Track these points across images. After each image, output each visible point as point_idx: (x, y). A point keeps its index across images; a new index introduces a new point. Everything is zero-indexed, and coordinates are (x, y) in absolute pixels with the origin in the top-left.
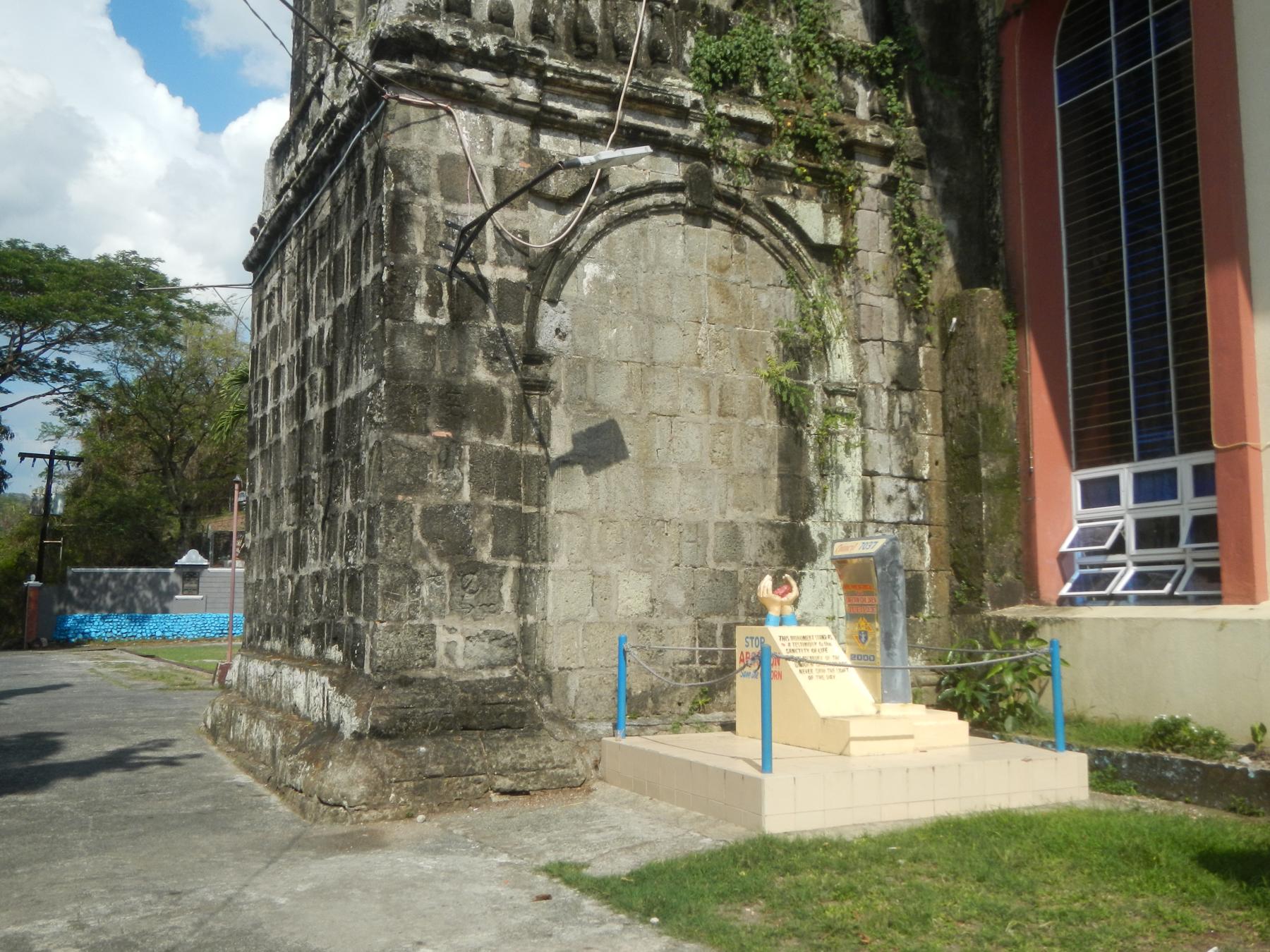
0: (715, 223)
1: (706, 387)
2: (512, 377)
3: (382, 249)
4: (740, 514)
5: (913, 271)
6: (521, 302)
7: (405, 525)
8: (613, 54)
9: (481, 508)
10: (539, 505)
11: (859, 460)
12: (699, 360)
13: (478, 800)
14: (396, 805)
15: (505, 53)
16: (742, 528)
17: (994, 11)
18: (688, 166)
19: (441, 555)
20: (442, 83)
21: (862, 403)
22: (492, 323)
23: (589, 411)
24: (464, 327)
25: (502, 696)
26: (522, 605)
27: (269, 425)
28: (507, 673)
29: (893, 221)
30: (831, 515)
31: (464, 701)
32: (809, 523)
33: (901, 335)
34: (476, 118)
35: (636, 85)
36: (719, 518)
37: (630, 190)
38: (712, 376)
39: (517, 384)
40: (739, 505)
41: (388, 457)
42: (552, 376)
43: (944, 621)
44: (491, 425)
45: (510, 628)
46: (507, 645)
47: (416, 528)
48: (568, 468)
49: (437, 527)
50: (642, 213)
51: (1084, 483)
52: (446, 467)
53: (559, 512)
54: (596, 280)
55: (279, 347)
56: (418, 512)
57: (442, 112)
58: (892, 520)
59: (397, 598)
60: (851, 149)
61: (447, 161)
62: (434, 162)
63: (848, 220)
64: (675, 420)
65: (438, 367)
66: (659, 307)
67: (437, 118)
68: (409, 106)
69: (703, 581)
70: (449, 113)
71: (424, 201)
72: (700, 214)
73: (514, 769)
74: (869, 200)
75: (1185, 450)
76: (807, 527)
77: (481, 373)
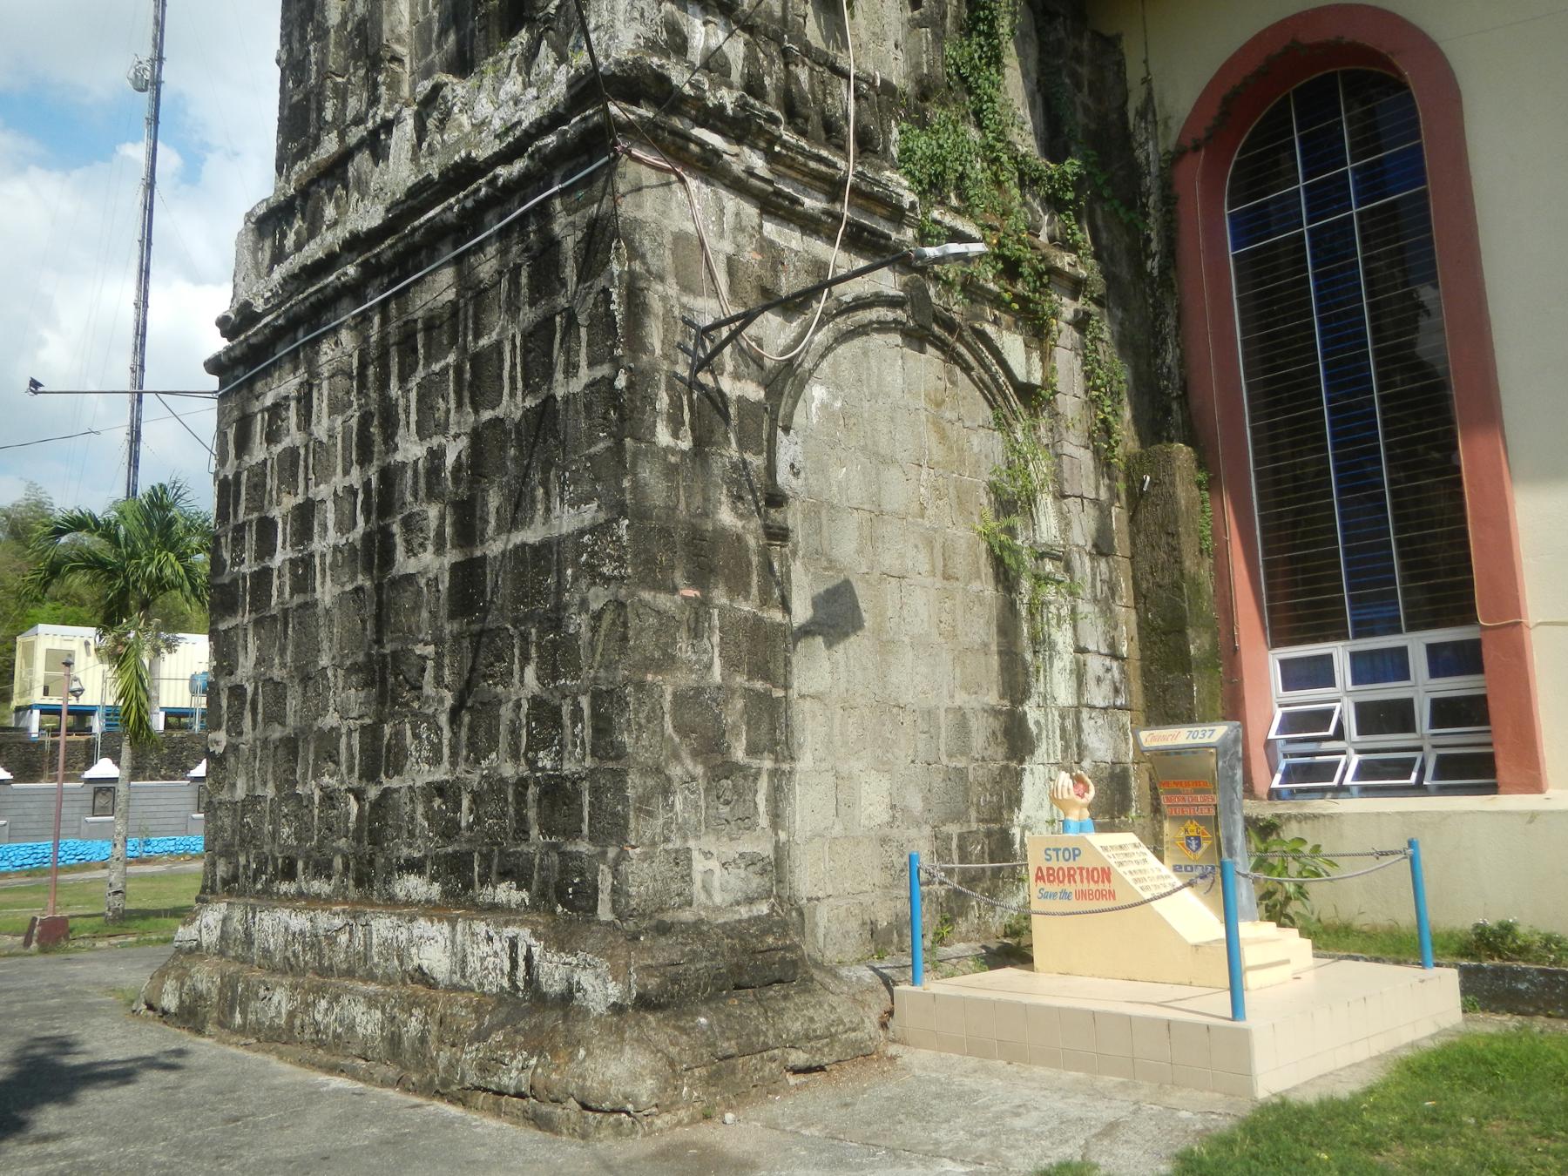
0: (929, 349)
1: (930, 543)
2: (756, 522)
3: (614, 346)
4: (965, 697)
5: (1104, 421)
6: (760, 427)
7: (655, 716)
8: (823, 136)
9: (733, 692)
11: (1069, 633)
12: (923, 508)
13: (771, 1087)
14: (689, 1104)
15: (742, 115)
16: (969, 715)
17: (1156, 145)
18: (905, 278)
19: (695, 754)
20: (680, 141)
21: (1068, 568)
22: (733, 451)
23: (826, 569)
24: (706, 454)
25: (770, 940)
26: (776, 818)
28: (763, 908)
29: (1084, 364)
30: (1045, 698)
31: (732, 949)
32: (1026, 708)
33: (1097, 493)
34: (706, 189)
35: (860, 175)
36: (947, 703)
37: (856, 299)
38: (935, 530)
39: (761, 531)
40: (965, 688)
41: (633, 623)
42: (790, 523)
43: (1148, 820)
44: (738, 586)
45: (766, 849)
46: (763, 872)
47: (667, 718)
48: (810, 639)
49: (689, 716)
50: (862, 330)
51: (1283, 663)
52: (696, 637)
53: (802, 696)
54: (824, 406)
56: (668, 697)
57: (674, 178)
58: (1102, 704)
59: (650, 814)
60: (1050, 275)
61: (680, 238)
62: (667, 239)
63: (1046, 357)
64: (904, 582)
65: (682, 505)
67: (668, 184)
68: (639, 167)
69: (938, 782)
70: (682, 180)
71: (660, 288)
72: (917, 337)
73: (808, 1038)
74: (1065, 335)
75: (1412, 628)
76: (1025, 713)
77: (726, 516)
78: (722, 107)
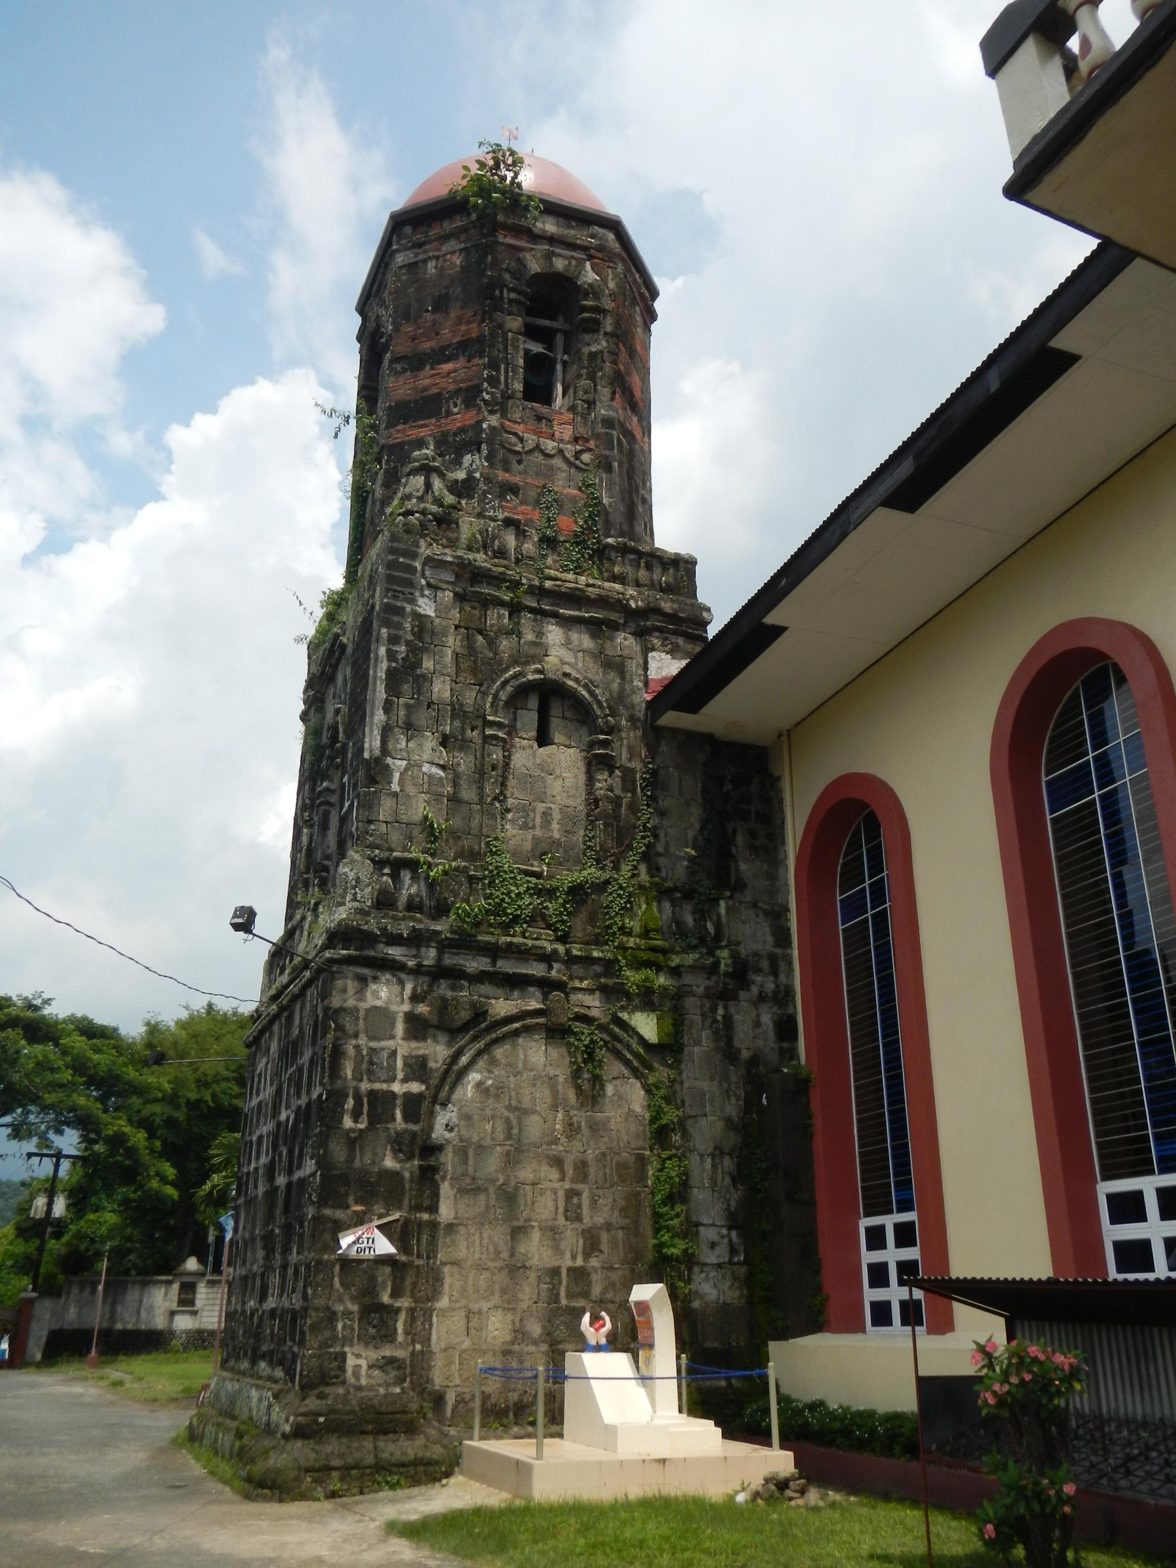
10: (428, 1258)
19: (353, 1299)
27: (251, 1181)
36: (569, 1263)
38: (566, 1151)
47: (336, 1279)
50: (516, 1033)
54: (479, 1085)
55: (262, 1120)
58: (715, 1261)
66: (526, 1102)
71: (354, 1042)
77: (389, 1163)
78: (401, 935)
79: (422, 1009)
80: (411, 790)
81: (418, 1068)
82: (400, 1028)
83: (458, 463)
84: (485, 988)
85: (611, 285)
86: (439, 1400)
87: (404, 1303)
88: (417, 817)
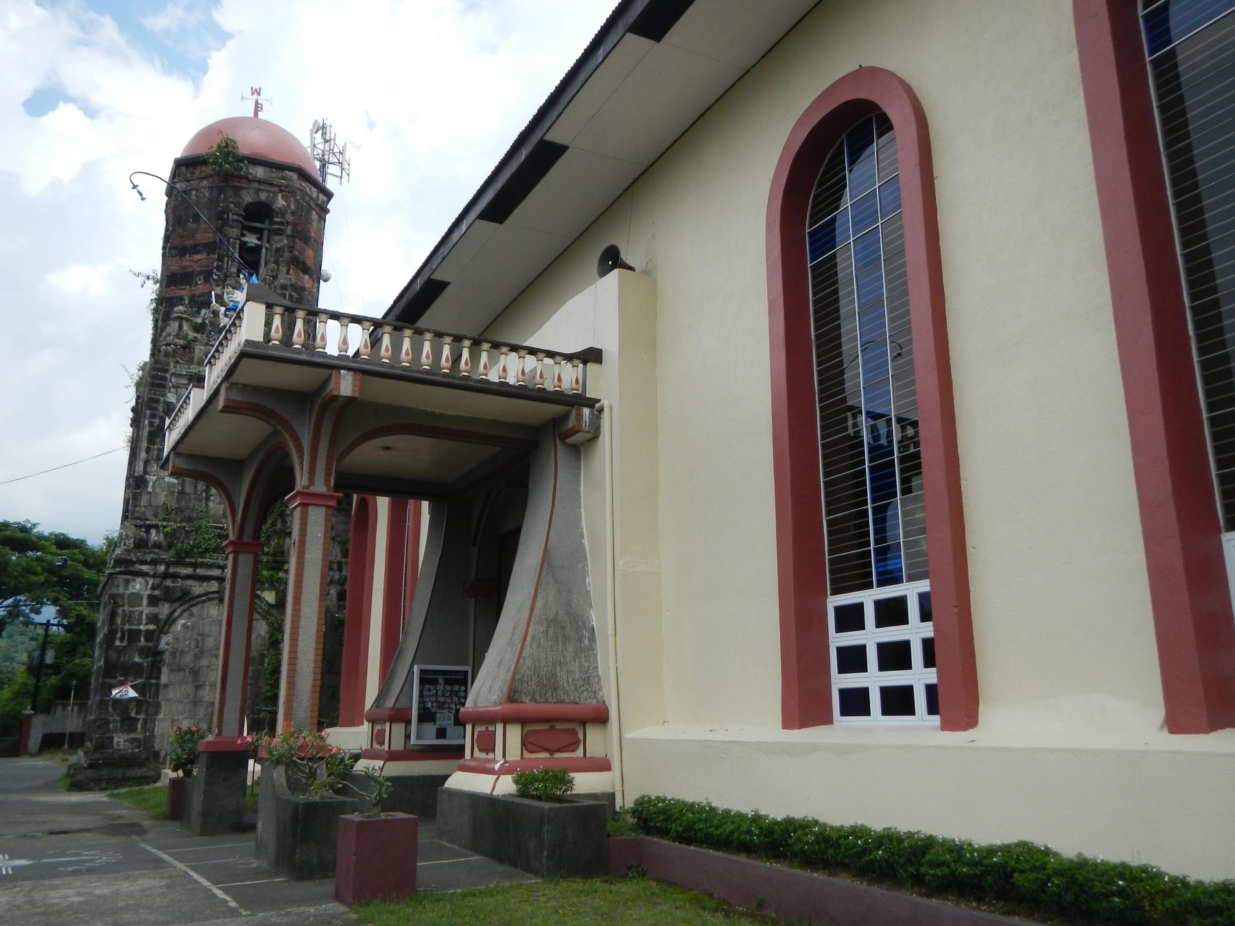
50: (204, 602)
54: (184, 625)
66: (207, 631)
77: (137, 659)
79: (156, 592)
80: (158, 490)
81: (153, 619)
82: (145, 602)
83: (198, 313)
84: (189, 582)
85: (293, 207)
86: (157, 755)
87: (142, 716)
88: (161, 503)
